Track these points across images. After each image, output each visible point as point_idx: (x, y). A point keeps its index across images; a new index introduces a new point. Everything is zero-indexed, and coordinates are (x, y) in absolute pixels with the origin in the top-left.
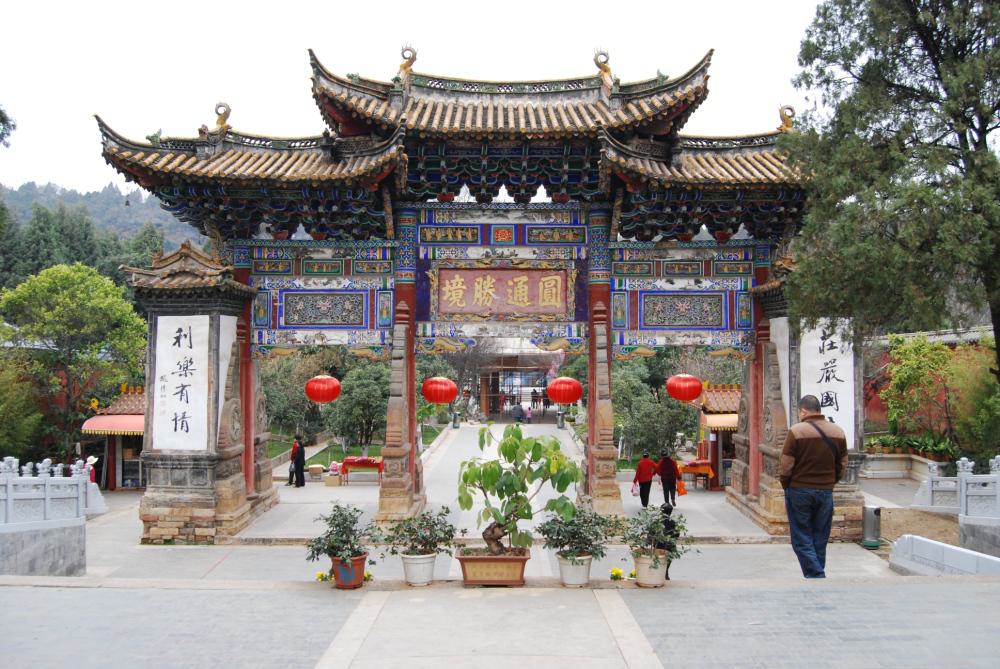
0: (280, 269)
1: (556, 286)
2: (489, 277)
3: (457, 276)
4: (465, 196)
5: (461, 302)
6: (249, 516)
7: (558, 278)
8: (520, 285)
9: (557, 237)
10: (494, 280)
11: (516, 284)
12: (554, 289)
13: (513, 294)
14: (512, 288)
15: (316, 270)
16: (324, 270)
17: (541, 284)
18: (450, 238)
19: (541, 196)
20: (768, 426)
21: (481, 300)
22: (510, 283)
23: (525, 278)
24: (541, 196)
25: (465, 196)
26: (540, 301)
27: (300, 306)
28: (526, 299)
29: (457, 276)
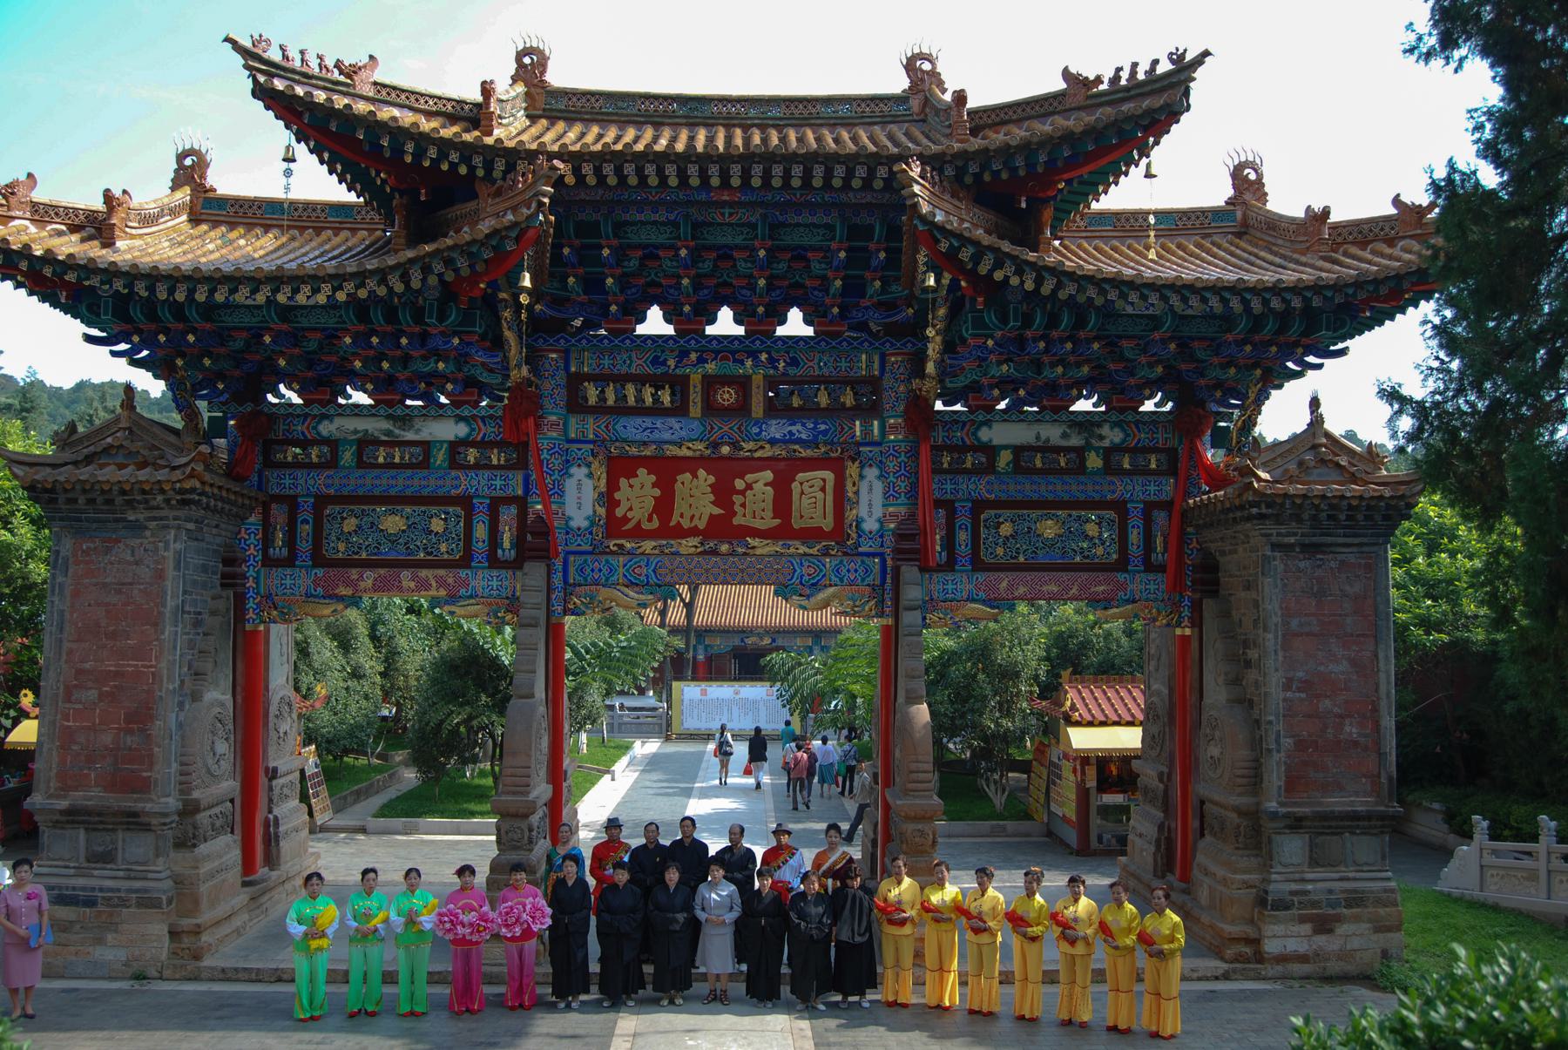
0: (315, 460)
1: (823, 489)
2: (702, 473)
3: (642, 472)
4: (655, 323)
5: (650, 519)
6: (246, 917)
7: (829, 476)
8: (759, 486)
9: (823, 399)
10: (712, 479)
11: (749, 487)
12: (820, 495)
13: (743, 505)
14: (743, 493)
15: (381, 460)
16: (397, 460)
17: (795, 486)
18: (631, 401)
19: (795, 325)
20: (1214, 751)
21: (688, 515)
22: (739, 484)
23: (768, 475)
24: (795, 325)
25: (655, 323)
26: (795, 514)
27: (350, 524)
28: (769, 513)
29: (642, 472)
